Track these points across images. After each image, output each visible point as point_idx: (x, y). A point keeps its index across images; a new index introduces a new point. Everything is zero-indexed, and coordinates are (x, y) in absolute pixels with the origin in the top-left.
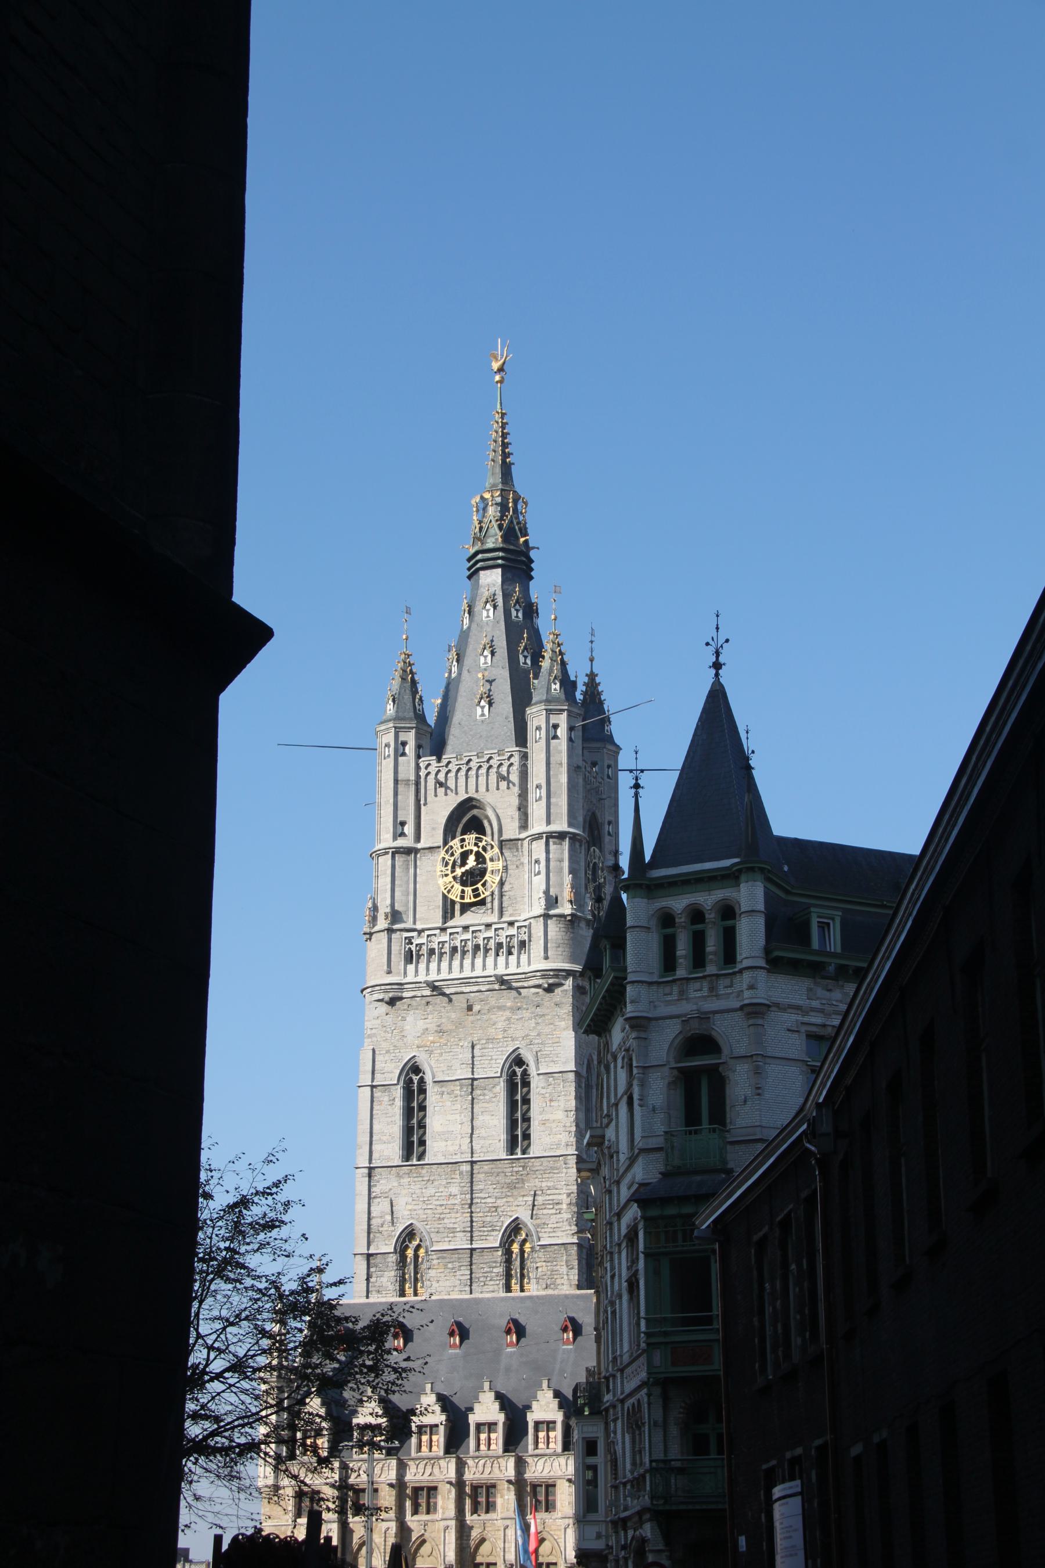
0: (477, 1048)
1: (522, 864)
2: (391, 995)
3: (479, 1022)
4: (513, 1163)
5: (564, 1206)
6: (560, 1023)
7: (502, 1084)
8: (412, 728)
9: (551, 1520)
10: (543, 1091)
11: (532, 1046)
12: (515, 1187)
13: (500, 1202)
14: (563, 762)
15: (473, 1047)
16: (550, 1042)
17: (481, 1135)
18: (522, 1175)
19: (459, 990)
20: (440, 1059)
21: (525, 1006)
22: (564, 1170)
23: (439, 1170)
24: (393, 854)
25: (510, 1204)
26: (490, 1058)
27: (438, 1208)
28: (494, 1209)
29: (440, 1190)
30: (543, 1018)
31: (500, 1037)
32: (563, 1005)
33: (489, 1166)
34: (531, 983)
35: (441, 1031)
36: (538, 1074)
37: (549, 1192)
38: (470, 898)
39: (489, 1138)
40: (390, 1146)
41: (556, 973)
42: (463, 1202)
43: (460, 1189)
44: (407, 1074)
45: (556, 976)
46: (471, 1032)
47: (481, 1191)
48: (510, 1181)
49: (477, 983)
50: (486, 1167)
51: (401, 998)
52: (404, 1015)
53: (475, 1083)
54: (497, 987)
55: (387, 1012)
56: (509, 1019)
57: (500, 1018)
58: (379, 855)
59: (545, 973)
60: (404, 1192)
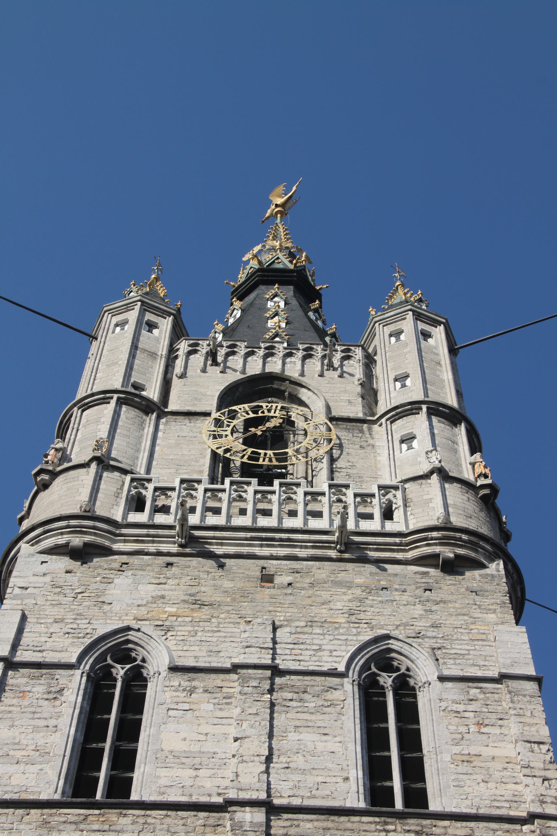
0: (279, 633)
1: (373, 446)
2: (88, 538)
3: (291, 597)
4: (386, 823)
6: (485, 615)
8: (169, 314)
11: (419, 640)
14: (443, 363)
15: (275, 629)
16: (467, 638)
17: (291, 765)
19: (245, 550)
20: (191, 639)
21: (397, 587)
23: (168, 820)
24: (120, 402)
26: (317, 647)
30: (442, 605)
31: (342, 620)
32: (487, 594)
36: (442, 679)
38: (270, 460)
39: (314, 772)
41: (473, 539)
44: (102, 658)
45: (472, 545)
46: (270, 609)
49: (290, 543)
50: (309, 825)
52: (112, 576)
53: (278, 680)
54: (333, 554)
55: (69, 568)
58: (87, 407)
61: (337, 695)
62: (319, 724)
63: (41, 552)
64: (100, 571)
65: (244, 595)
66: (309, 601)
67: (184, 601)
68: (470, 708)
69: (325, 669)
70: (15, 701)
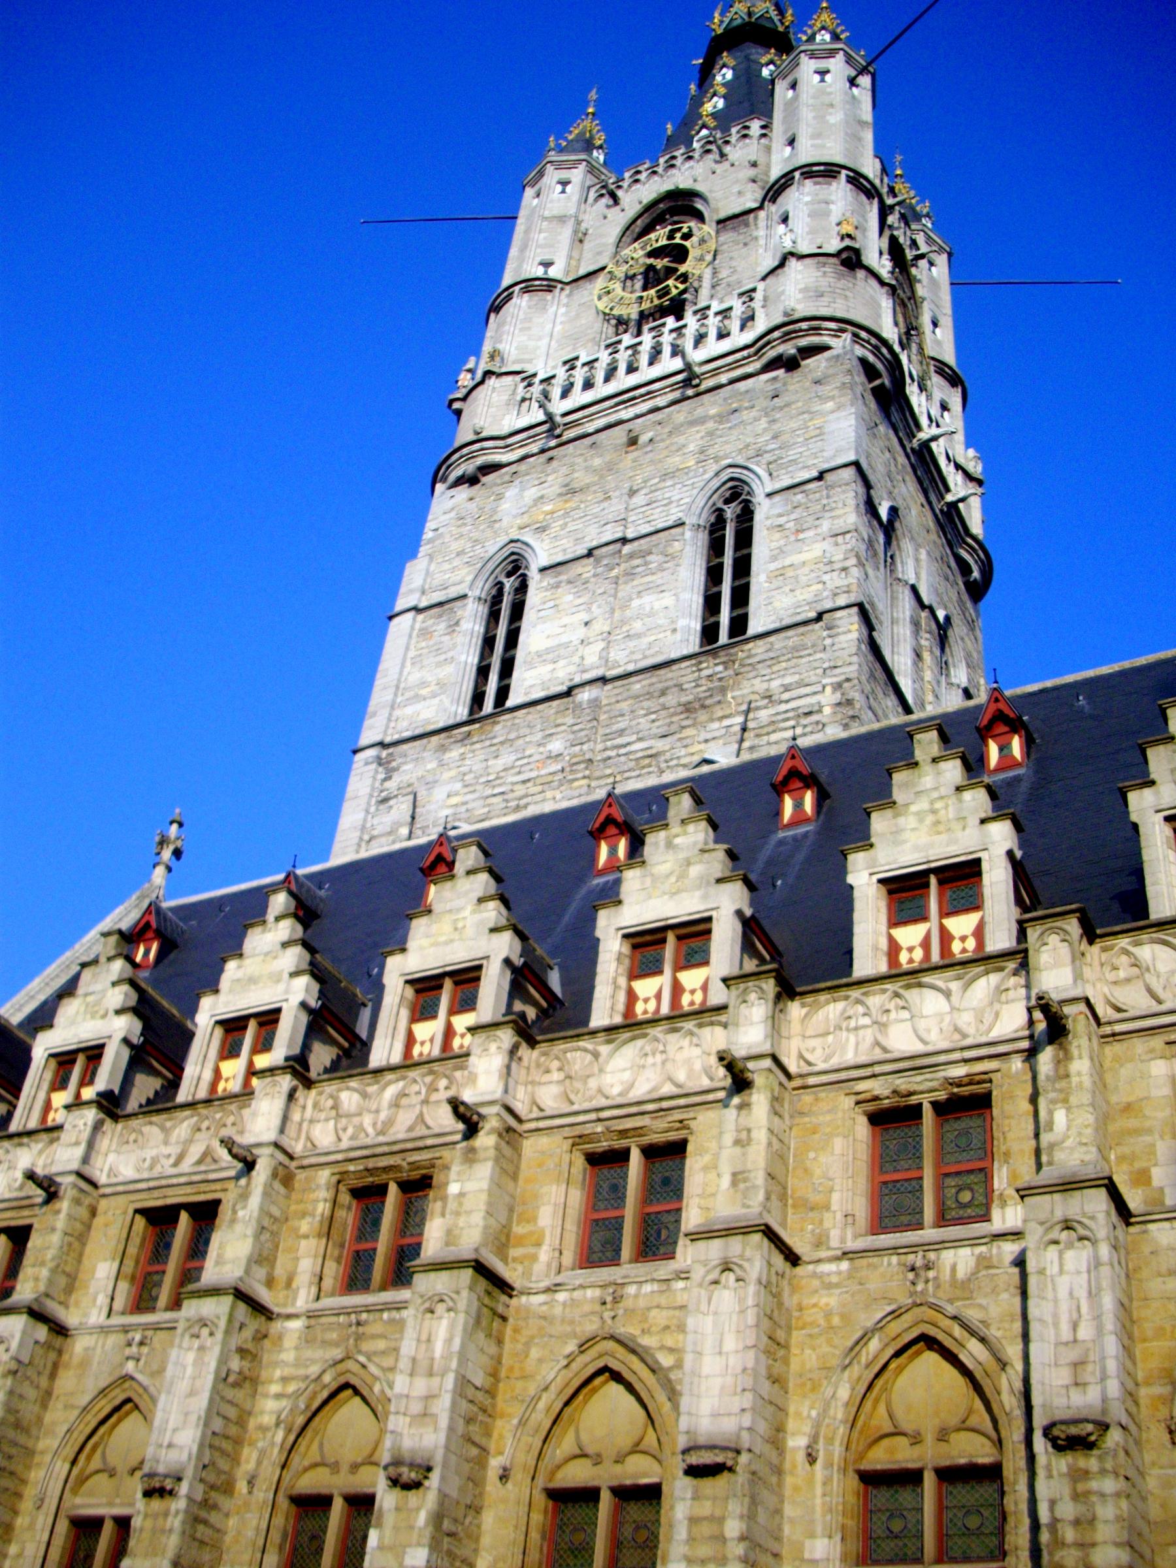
5: (827, 710)
7: (688, 534)
9: (647, 1288)
10: (782, 520)
12: (703, 707)
13: (660, 745)
18: (720, 679)
22: (828, 642)
23: (530, 717)
25: (685, 742)
27: (516, 787)
28: (647, 761)
29: (528, 753)
33: (645, 683)
34: (758, 365)
35: (570, 491)
37: (786, 696)
40: (436, 701)
42: (575, 760)
43: (571, 737)
47: (621, 733)
48: (690, 698)
50: (638, 686)
51: (495, 467)
56: (711, 434)
57: (693, 440)
59: (788, 327)
60: (447, 775)
61: (677, 545)
62: (660, 582)
63: (450, 487)
64: (495, 489)
65: (610, 468)
66: (665, 453)
67: (560, 495)
68: (793, 517)
69: (670, 523)
70: (423, 644)
